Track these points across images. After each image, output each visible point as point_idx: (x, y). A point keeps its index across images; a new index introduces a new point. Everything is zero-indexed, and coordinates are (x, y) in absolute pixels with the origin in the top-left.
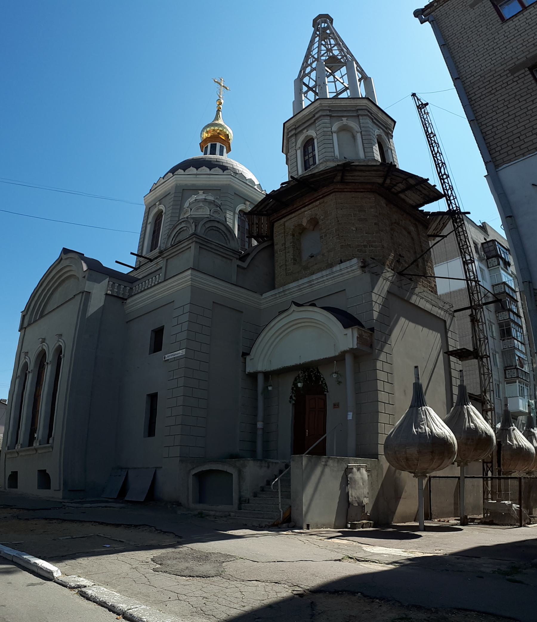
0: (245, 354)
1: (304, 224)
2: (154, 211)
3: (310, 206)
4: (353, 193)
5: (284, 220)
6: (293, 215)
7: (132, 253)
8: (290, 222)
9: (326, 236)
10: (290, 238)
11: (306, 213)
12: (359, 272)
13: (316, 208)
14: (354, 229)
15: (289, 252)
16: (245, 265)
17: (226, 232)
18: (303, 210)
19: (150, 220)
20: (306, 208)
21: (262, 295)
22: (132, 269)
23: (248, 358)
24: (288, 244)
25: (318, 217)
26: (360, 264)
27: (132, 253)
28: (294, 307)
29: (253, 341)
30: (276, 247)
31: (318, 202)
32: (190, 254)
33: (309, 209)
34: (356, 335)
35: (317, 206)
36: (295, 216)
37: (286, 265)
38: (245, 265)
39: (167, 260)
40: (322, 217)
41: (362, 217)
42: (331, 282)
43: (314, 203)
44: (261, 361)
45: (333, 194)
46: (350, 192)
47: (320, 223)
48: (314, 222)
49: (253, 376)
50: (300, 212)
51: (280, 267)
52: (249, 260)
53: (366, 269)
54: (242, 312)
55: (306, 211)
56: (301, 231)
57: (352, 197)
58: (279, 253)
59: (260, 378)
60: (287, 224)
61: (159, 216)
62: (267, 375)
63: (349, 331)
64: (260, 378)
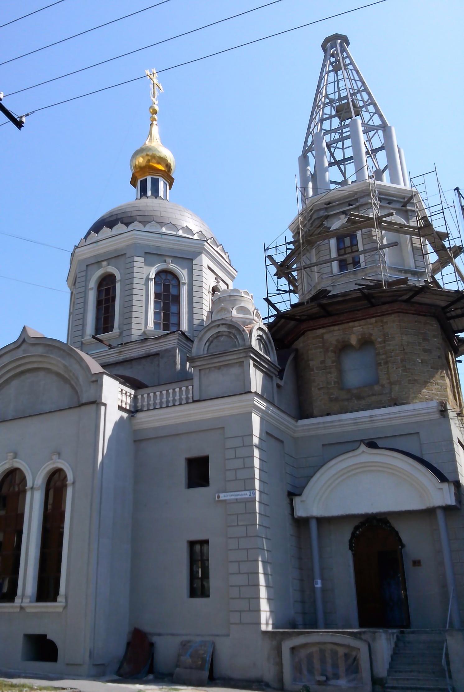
0: (291, 495)
3: (362, 322)
4: (415, 316)
6: (336, 328)
8: (333, 335)
9: (386, 363)
11: (355, 328)
13: (370, 326)
14: (420, 361)
15: (330, 373)
17: (267, 342)
18: (351, 324)
20: (356, 323)
21: (297, 421)
24: (329, 363)
28: (363, 448)
31: (373, 320)
33: (360, 326)
35: (371, 324)
36: (339, 330)
38: (281, 383)
39: (200, 370)
40: (379, 340)
41: (427, 347)
42: (400, 421)
43: (368, 320)
44: (316, 502)
45: (396, 315)
46: (413, 314)
48: (366, 343)
50: (346, 325)
51: (319, 389)
55: (355, 327)
56: (344, 347)
57: (416, 322)
58: (316, 371)
59: (313, 525)
60: (326, 337)
62: (321, 521)
64: (313, 525)
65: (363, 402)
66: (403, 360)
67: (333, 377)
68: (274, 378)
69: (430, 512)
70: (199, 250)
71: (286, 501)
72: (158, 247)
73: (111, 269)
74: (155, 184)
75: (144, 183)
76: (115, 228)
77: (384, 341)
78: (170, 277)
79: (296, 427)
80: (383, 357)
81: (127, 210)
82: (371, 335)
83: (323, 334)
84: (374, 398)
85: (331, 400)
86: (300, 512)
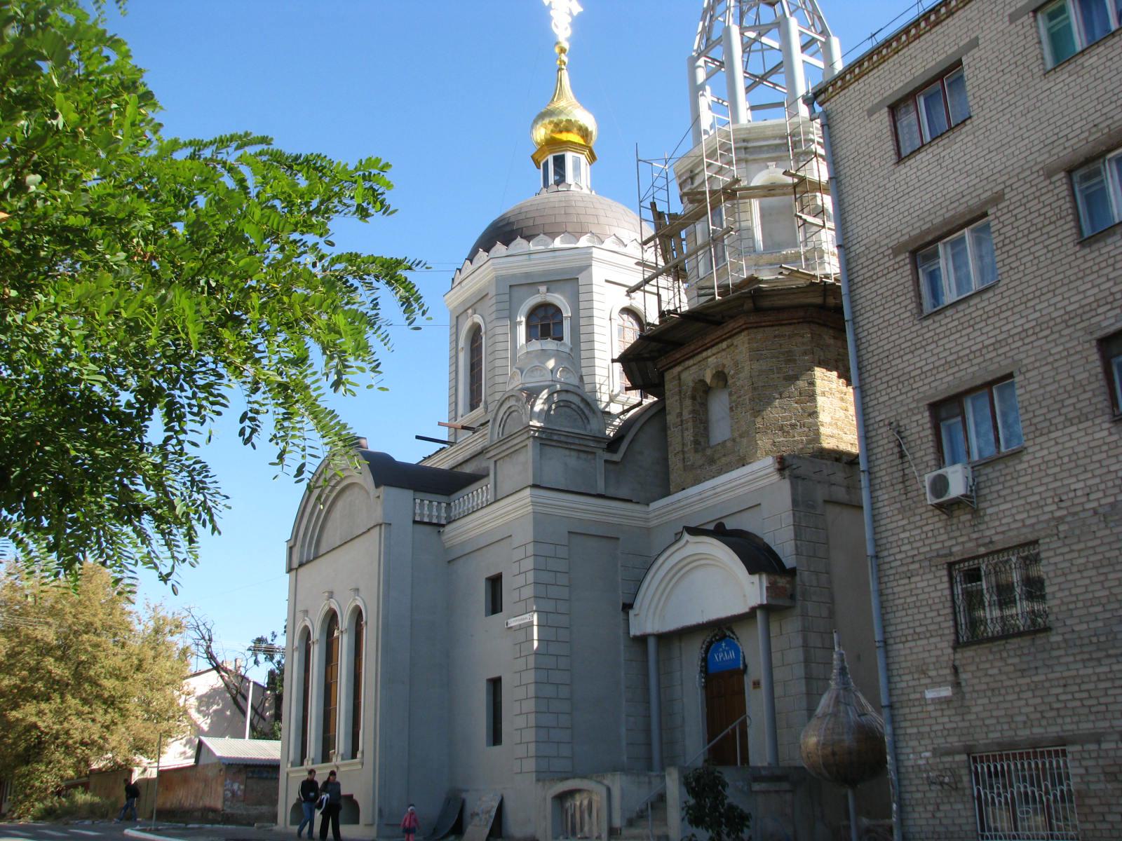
0: (627, 607)
1: (708, 381)
2: (466, 326)
3: (715, 350)
5: (679, 369)
6: (691, 362)
7: (440, 424)
10: (688, 402)
12: (776, 477)
16: (616, 457)
17: (582, 406)
18: (704, 354)
19: (462, 343)
20: (709, 352)
22: (439, 446)
23: (631, 613)
24: (686, 415)
25: (726, 371)
26: (777, 466)
27: (440, 424)
28: (687, 537)
29: (639, 582)
30: (669, 418)
31: (724, 345)
32: (528, 455)
34: (765, 584)
37: (683, 452)
38: (616, 457)
41: (791, 373)
45: (745, 333)
47: (730, 381)
48: (721, 377)
49: (642, 640)
52: (623, 447)
53: (787, 473)
54: (617, 539)
59: (652, 643)
60: (684, 376)
61: (476, 334)
63: (756, 578)
64: (652, 643)
65: (714, 467)
66: (752, 400)
67: (689, 436)
68: (600, 452)
69: (753, 612)
70: (584, 263)
71: (621, 615)
72: (527, 275)
73: (478, 319)
74: (560, 162)
75: (546, 164)
76: (512, 245)
77: (736, 373)
78: (541, 313)
79: (648, 513)
80: (734, 397)
81: (512, 220)
82: (724, 366)
83: (680, 373)
84: (724, 460)
85: (685, 468)
86: (635, 631)
